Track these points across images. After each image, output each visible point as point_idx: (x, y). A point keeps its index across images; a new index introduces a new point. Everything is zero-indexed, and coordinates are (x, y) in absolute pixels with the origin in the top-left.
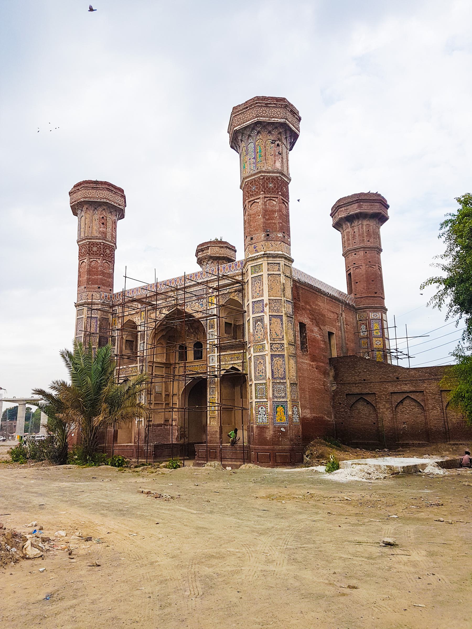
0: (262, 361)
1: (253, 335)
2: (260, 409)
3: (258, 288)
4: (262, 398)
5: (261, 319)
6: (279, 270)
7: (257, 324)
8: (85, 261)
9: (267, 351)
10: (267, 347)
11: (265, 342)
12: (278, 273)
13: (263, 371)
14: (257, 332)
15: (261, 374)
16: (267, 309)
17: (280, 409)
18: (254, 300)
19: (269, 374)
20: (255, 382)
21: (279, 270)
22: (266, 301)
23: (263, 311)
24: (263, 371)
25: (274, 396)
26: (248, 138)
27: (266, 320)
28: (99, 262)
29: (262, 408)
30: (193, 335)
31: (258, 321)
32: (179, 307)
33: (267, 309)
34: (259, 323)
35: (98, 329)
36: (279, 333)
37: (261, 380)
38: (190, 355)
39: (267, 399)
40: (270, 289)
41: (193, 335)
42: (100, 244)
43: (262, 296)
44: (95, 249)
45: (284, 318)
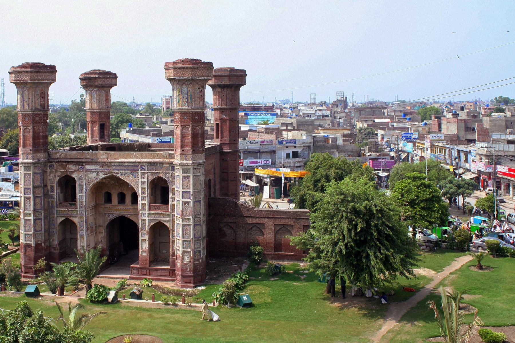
6: (200, 172)
9: (191, 222)
10: (192, 220)
11: (191, 217)
12: (199, 174)
18: (184, 190)
19: (192, 236)
20: (183, 239)
21: (200, 172)
22: (191, 193)
23: (190, 198)
25: (195, 248)
27: (191, 204)
30: (117, 187)
32: (114, 174)
33: (191, 197)
36: (198, 211)
40: (195, 184)
41: (117, 187)
43: (190, 189)
45: (202, 202)
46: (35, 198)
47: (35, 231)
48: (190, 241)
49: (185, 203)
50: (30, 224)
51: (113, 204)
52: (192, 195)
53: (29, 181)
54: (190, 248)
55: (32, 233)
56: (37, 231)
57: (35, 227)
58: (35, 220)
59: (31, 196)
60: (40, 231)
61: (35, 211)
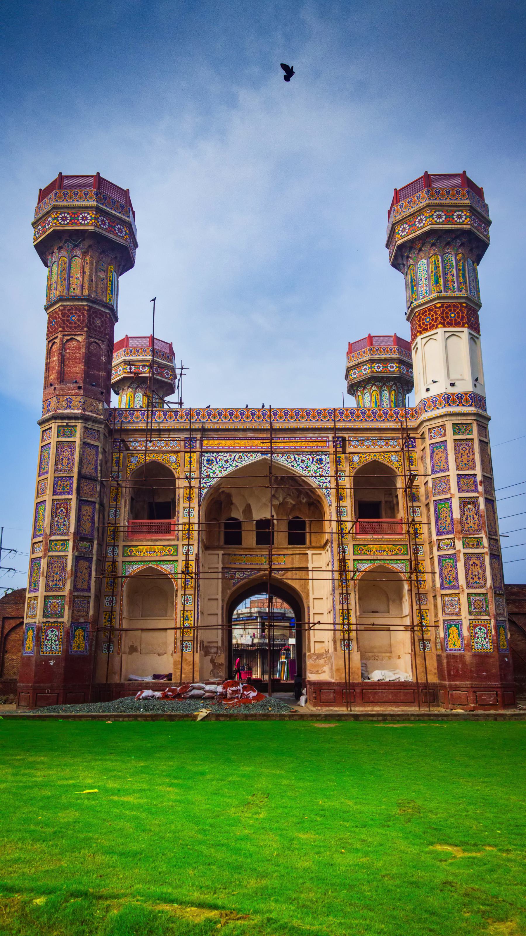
0: (477, 562)
1: (461, 523)
2: (477, 630)
3: (465, 458)
4: (479, 614)
5: (474, 502)
7: (466, 507)
8: (79, 338)
11: (483, 535)
13: (481, 576)
14: (467, 519)
15: (476, 579)
16: (480, 488)
17: (453, 631)
18: (461, 472)
19: (489, 582)
20: (467, 591)
22: (479, 478)
23: (476, 490)
24: (481, 576)
26: (446, 246)
28: (103, 346)
29: (480, 629)
31: (469, 503)
33: (480, 488)
34: (469, 506)
35: (99, 468)
37: (475, 588)
38: (249, 538)
39: (489, 616)
42: (106, 317)
43: (473, 468)
44: (98, 322)
46: (81, 502)
47: (75, 587)
48: (485, 595)
49: (464, 503)
50: (63, 569)
51: (244, 545)
52: (481, 482)
53: (71, 461)
54: (487, 614)
55: (66, 593)
56: (78, 590)
57: (76, 577)
58: (77, 559)
59: (73, 497)
60: (84, 590)
61: (80, 537)
